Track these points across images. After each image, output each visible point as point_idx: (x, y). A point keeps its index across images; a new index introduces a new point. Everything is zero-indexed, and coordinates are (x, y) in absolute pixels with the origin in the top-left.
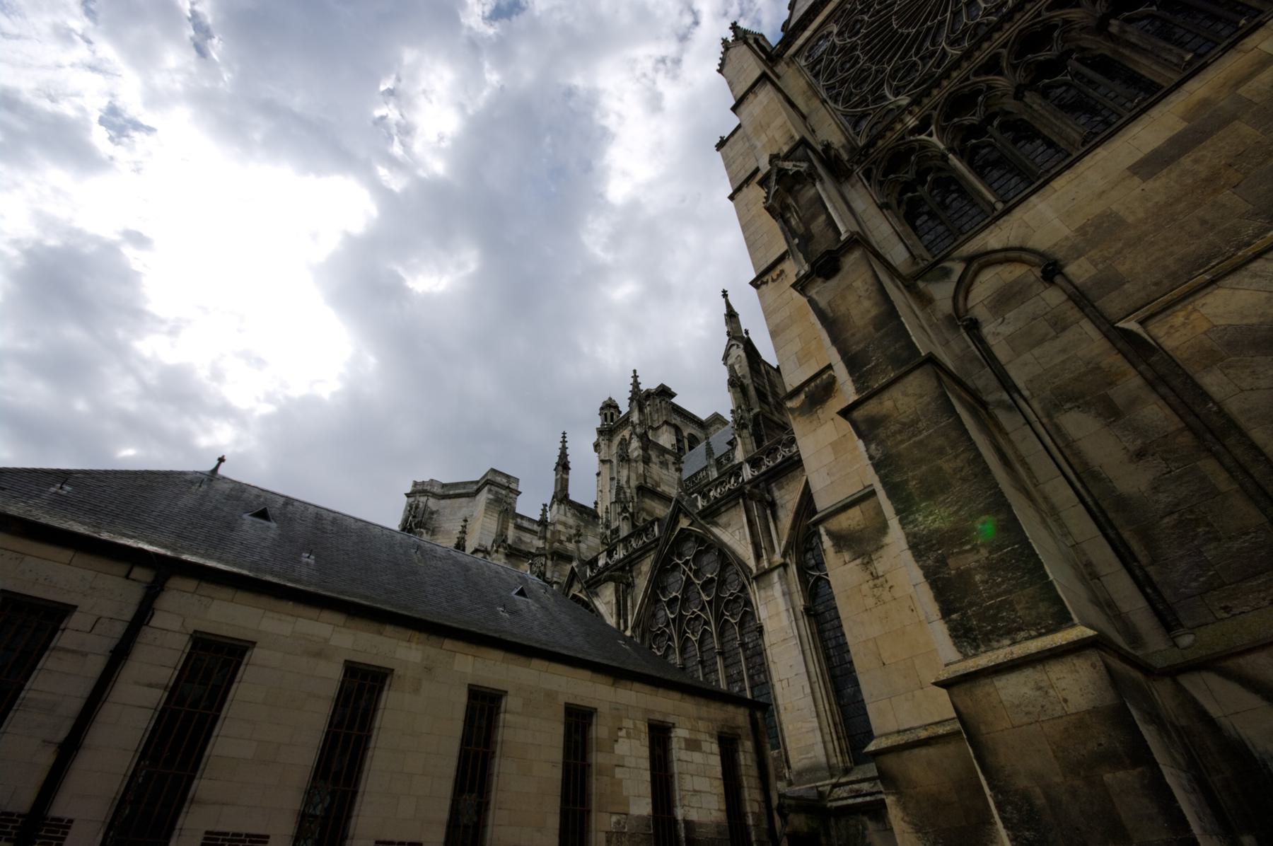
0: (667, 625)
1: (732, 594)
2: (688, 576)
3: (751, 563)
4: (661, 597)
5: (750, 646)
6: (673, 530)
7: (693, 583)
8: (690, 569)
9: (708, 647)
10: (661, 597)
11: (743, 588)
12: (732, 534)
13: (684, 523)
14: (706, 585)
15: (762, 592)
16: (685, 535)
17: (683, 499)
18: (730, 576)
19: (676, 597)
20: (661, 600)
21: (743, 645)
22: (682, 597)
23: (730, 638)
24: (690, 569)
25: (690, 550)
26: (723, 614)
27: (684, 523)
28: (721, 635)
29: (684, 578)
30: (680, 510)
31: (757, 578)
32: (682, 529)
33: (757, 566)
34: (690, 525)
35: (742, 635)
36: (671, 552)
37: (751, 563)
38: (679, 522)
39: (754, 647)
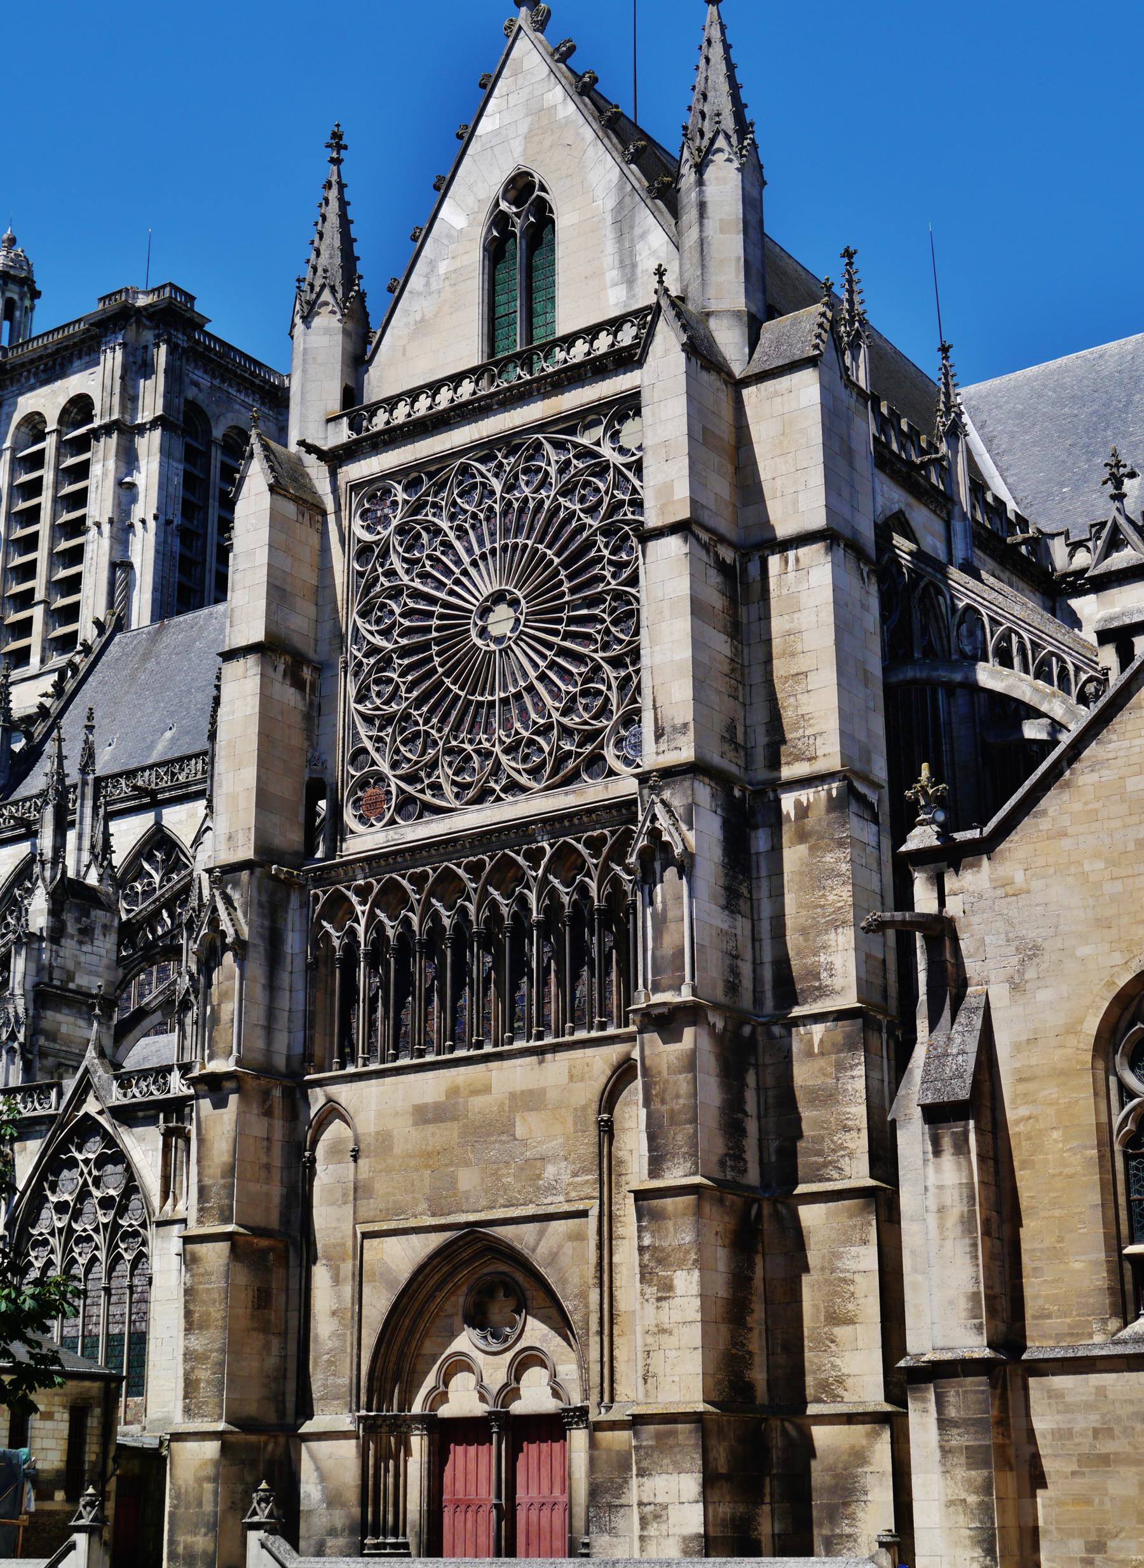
0: (52, 1234)
1: (131, 1226)
2: (85, 1184)
3: (156, 1200)
4: (48, 1193)
5: (139, 1289)
6: (78, 1108)
7: (90, 1194)
8: (90, 1173)
9: (95, 1276)
10: (48, 1193)
11: (143, 1225)
12: (145, 1152)
13: (91, 1106)
14: (106, 1203)
15: (159, 1240)
16: (88, 1128)
17: (96, 1072)
18: (134, 1203)
19: (66, 1202)
20: (46, 1196)
21: (131, 1287)
22: (75, 1205)
23: (120, 1274)
24: (90, 1173)
25: (93, 1149)
26: (117, 1246)
27: (91, 1106)
28: (111, 1269)
29: (81, 1182)
30: (89, 1085)
31: (160, 1224)
32: (86, 1114)
33: (161, 1208)
34: (101, 1113)
35: (132, 1275)
36: (68, 1139)
37: (156, 1200)
38: (84, 1101)
39: (142, 1292)
